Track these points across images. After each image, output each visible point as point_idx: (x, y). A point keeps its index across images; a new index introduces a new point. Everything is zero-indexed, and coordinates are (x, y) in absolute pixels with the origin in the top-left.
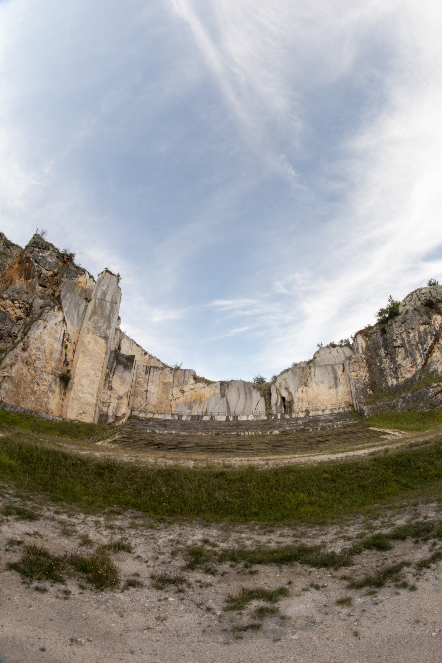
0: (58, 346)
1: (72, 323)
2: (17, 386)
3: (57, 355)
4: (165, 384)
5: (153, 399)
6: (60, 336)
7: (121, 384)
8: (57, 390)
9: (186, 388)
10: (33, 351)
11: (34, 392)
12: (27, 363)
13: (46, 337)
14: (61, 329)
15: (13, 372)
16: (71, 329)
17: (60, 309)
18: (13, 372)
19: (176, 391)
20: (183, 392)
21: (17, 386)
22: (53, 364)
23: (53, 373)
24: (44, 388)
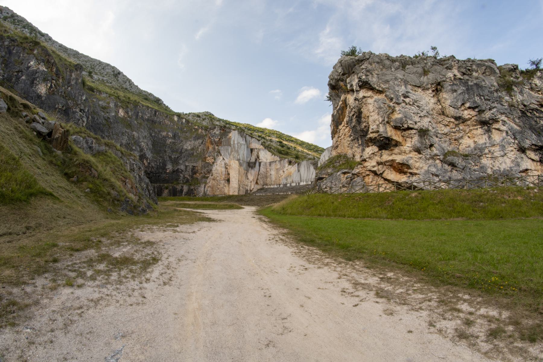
0: (224, 169)
1: (227, 158)
2: (212, 188)
3: (224, 173)
4: (277, 169)
5: (273, 178)
6: (223, 165)
7: (252, 175)
8: (227, 185)
9: (285, 170)
10: (215, 175)
11: (218, 188)
12: (214, 180)
13: (219, 168)
14: (223, 163)
15: (210, 184)
16: (227, 161)
17: (221, 155)
18: (210, 184)
19: (281, 172)
20: (284, 172)
21: (212, 188)
22: (223, 176)
23: (224, 180)
24: (221, 186)
